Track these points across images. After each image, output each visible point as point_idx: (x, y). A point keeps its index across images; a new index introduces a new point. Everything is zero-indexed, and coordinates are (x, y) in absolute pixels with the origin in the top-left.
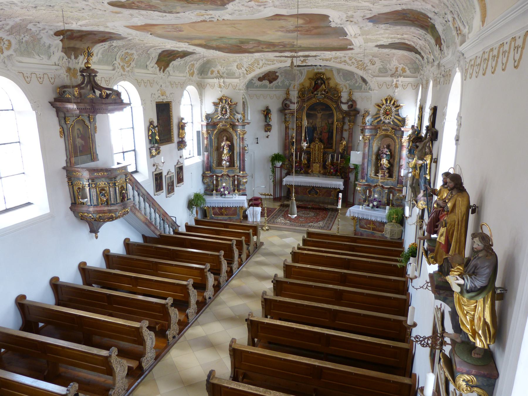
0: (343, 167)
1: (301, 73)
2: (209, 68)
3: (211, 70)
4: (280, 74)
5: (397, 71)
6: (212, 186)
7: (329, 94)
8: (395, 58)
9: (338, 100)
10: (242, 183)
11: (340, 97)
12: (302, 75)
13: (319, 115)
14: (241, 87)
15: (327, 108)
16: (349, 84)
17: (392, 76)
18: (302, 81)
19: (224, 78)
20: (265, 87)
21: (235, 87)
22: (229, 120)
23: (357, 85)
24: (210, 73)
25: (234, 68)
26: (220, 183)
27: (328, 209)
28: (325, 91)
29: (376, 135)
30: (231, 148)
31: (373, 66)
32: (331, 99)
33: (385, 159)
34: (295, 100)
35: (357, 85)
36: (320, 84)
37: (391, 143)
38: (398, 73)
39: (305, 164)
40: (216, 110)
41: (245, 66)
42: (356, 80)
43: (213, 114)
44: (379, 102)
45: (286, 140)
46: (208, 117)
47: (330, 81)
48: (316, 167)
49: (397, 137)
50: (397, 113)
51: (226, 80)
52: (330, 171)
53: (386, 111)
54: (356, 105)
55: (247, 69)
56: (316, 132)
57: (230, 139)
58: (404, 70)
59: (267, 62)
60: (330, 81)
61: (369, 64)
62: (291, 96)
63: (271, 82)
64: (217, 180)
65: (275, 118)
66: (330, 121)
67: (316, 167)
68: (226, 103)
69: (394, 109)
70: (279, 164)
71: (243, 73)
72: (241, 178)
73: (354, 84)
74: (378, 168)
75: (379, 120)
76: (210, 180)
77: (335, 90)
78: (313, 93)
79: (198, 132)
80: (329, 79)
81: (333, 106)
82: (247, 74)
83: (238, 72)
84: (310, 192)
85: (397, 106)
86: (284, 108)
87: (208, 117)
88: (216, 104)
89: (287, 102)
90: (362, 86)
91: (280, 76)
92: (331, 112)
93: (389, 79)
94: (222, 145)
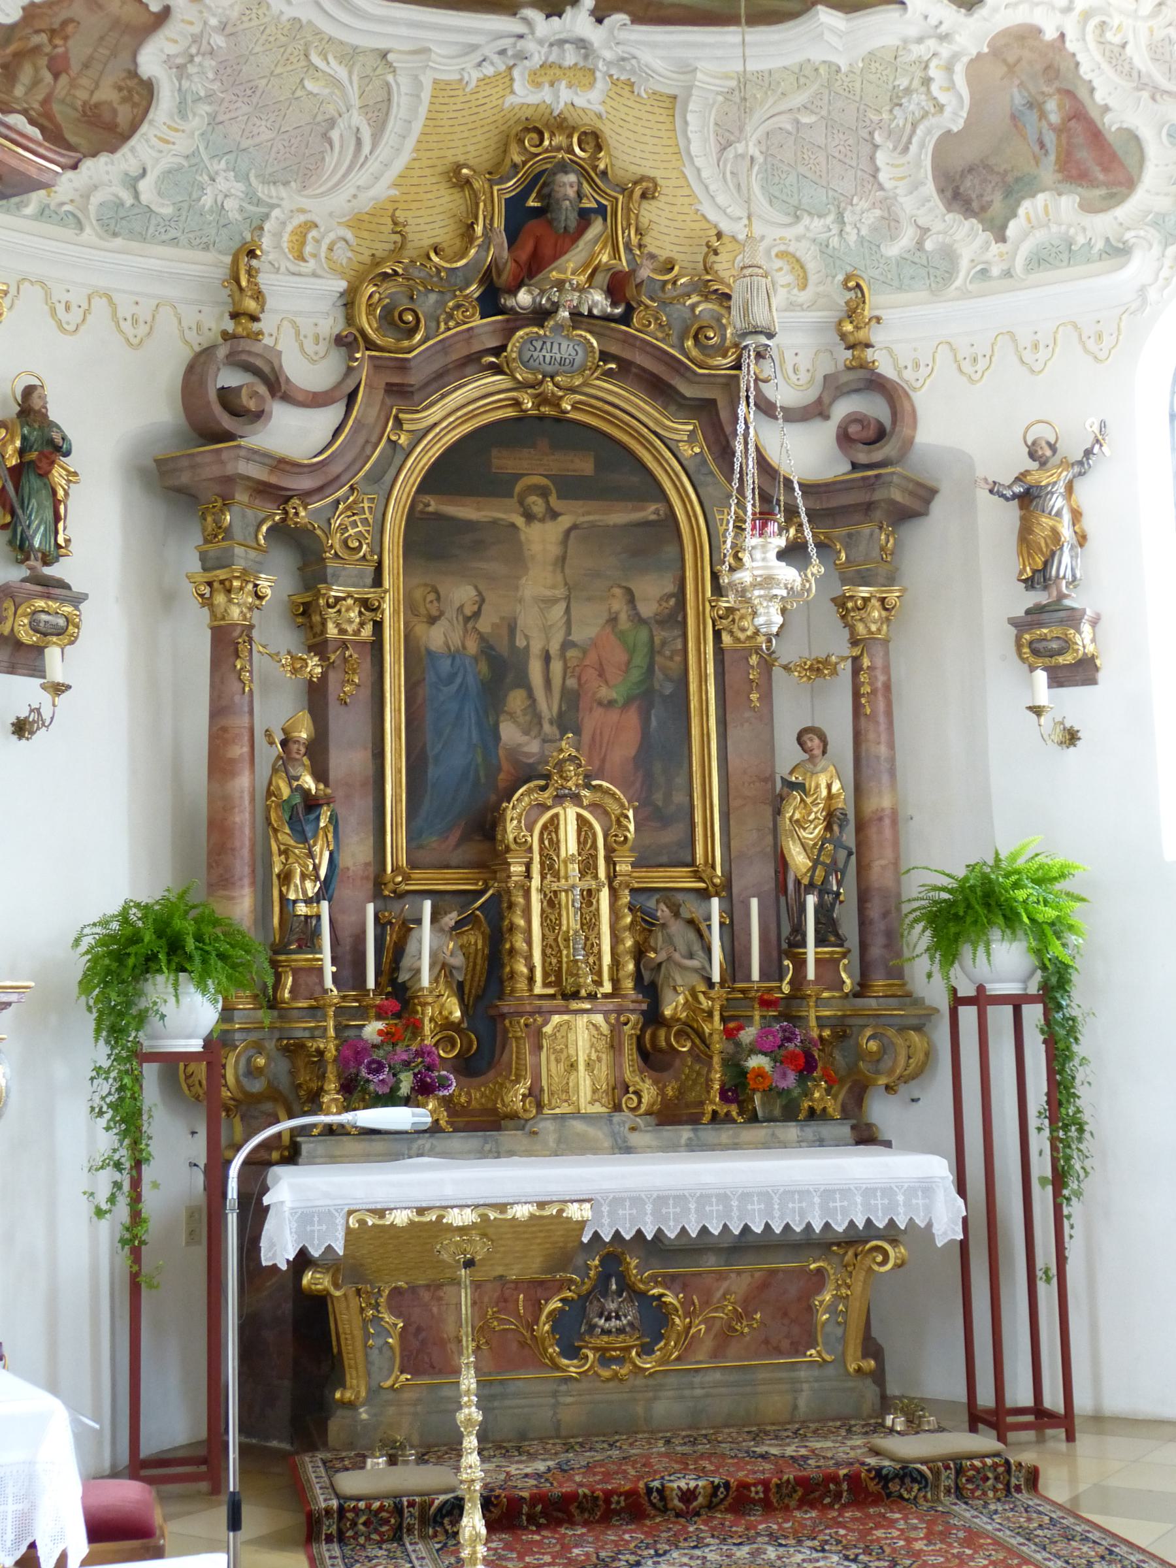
1: (379, 112)
12: (379, 129)
13: (541, 539)
15: (615, 469)
18: (382, 190)
23: (892, 250)
27: (907, 1474)
32: (658, 389)
34: (308, 364)
36: (567, 215)
45: (219, 765)
47: (649, 212)
48: (579, 1046)
56: (516, 700)
60: (649, 212)
66: (651, 592)
67: (579, 1046)
70: (188, 1015)
73: (870, 245)
84: (571, 1332)
90: (949, 255)
92: (650, 512)
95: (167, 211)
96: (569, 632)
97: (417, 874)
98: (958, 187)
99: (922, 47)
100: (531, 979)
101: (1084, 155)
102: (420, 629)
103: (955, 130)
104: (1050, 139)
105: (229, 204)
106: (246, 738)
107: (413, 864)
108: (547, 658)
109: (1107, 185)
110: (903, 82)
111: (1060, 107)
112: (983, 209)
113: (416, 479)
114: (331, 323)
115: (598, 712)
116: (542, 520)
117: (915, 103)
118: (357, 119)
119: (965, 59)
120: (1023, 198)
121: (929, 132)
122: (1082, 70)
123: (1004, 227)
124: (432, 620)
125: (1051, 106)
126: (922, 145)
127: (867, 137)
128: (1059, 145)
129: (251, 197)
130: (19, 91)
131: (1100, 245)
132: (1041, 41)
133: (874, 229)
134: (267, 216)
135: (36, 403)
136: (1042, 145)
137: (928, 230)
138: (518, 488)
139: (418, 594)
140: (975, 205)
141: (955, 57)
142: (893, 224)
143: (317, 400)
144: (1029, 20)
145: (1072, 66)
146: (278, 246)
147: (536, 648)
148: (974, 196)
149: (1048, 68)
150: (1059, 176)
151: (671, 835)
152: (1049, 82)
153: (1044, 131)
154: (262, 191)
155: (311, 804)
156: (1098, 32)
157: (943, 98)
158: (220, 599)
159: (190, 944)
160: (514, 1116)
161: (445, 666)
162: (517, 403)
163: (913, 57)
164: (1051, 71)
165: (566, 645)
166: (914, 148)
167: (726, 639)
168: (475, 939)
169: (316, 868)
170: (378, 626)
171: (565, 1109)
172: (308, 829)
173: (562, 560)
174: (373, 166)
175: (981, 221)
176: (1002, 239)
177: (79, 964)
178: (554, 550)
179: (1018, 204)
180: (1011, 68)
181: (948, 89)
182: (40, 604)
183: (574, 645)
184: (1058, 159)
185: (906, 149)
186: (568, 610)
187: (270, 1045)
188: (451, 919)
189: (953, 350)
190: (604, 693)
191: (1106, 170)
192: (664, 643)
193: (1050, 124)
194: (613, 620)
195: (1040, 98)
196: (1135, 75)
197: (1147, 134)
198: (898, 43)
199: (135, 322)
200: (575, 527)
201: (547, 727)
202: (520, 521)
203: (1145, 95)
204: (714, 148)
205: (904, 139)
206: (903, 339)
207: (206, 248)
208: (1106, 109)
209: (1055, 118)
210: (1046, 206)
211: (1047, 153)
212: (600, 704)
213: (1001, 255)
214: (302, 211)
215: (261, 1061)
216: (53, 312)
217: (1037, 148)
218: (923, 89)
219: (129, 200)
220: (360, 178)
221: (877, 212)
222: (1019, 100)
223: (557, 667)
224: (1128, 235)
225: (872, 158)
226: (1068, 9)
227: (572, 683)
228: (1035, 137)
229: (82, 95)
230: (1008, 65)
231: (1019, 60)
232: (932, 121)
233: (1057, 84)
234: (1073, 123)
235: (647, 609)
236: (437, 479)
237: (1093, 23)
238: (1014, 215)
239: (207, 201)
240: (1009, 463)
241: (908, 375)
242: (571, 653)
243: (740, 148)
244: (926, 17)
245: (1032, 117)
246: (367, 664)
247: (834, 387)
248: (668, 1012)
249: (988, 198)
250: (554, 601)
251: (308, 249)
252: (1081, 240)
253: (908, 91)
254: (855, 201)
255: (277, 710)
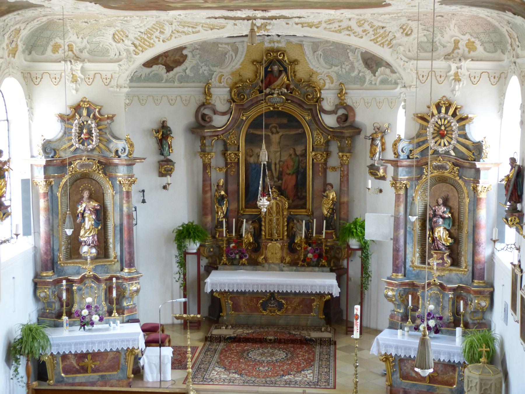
0: (332, 248)
1: (236, 51)
2: (50, 39)
3: (52, 43)
4: (191, 52)
5: (456, 47)
6: (57, 306)
7: (296, 94)
8: (454, 22)
9: (312, 103)
10: (127, 294)
11: (319, 100)
14: (121, 82)
15: (292, 122)
16: (337, 74)
17: (447, 57)
18: (238, 66)
19: (83, 61)
20: (157, 78)
21: (107, 82)
22: (96, 153)
23: (353, 75)
24: (50, 48)
25: (107, 40)
26: (77, 297)
27: (311, 340)
28: (287, 88)
29: (419, 179)
30: (101, 216)
31: (406, 39)
32: (300, 105)
33: (441, 229)
34: (221, 105)
35: (353, 75)
36: (276, 73)
37: (451, 195)
38: (460, 51)
39: (250, 244)
40: (67, 133)
41: (131, 36)
42: (352, 64)
43: (60, 140)
44: (422, 110)
45: (204, 192)
46: (48, 147)
47: (297, 68)
48: (274, 249)
49: (465, 181)
50: (461, 132)
51: (88, 65)
52: (306, 256)
53: (440, 128)
54: (354, 116)
55: (137, 43)
57: (97, 196)
58: (471, 46)
59: (181, 29)
61: (398, 35)
62: (214, 97)
63: (169, 69)
64: (69, 291)
65: (180, 147)
67: (274, 249)
68: (88, 115)
69: (455, 125)
70: (193, 247)
71: (127, 51)
72: (126, 284)
73: (348, 73)
74: (427, 247)
75: (424, 146)
76: (53, 292)
77: (309, 86)
78: (261, 92)
79: (25, 183)
80: (295, 62)
81: (305, 118)
82: (136, 54)
83: (114, 48)
84: (264, 306)
85: (462, 119)
86: (200, 125)
87: (48, 147)
88: (65, 119)
89: (207, 112)
90: (365, 78)
91: (190, 55)
92: (300, 131)
93: (440, 64)
94: (80, 209)
95: (192, 75)
96: (281, 158)
97: (247, 210)
100: (265, 236)
102: (248, 158)
105: (205, 72)
106: (209, 186)
107: (246, 208)
108: (276, 164)
113: (248, 125)
114: (227, 97)
115: (286, 176)
116: (275, 134)
118: (231, 53)
124: (251, 156)
129: (210, 70)
130: (159, 61)
131: (393, 81)
133: (349, 69)
134: (213, 74)
135: (165, 125)
138: (270, 126)
139: (248, 151)
143: (224, 114)
146: (215, 80)
147: (273, 162)
151: (301, 203)
154: (212, 68)
155: (223, 197)
158: (204, 158)
159: (192, 234)
160: (260, 263)
161: (254, 166)
162: (269, 109)
165: (280, 161)
167: (315, 160)
168: (257, 225)
169: (223, 212)
170: (239, 159)
171: (271, 262)
172: (222, 204)
173: (279, 143)
174: (236, 61)
176: (375, 76)
177: (175, 234)
178: (278, 140)
182: (166, 166)
183: (281, 161)
185: (354, 54)
186: (280, 154)
187: (214, 246)
188: (250, 222)
189: (364, 100)
190: (288, 172)
192: (302, 160)
194: (291, 155)
199: (186, 100)
200: (283, 135)
201: (275, 179)
202: (270, 134)
204: (311, 52)
206: (355, 97)
207: (200, 82)
212: (287, 174)
214: (221, 72)
215: (212, 250)
216: (169, 101)
219: (184, 74)
220: (233, 64)
223: (278, 166)
224: (398, 81)
227: (281, 169)
229: (172, 59)
235: (298, 153)
236: (251, 126)
239: (201, 72)
240: (369, 131)
241: (355, 104)
242: (281, 163)
243: (317, 53)
246: (236, 167)
247: (337, 107)
248: (296, 241)
250: (278, 152)
251: (222, 80)
252: (390, 79)
255: (218, 177)
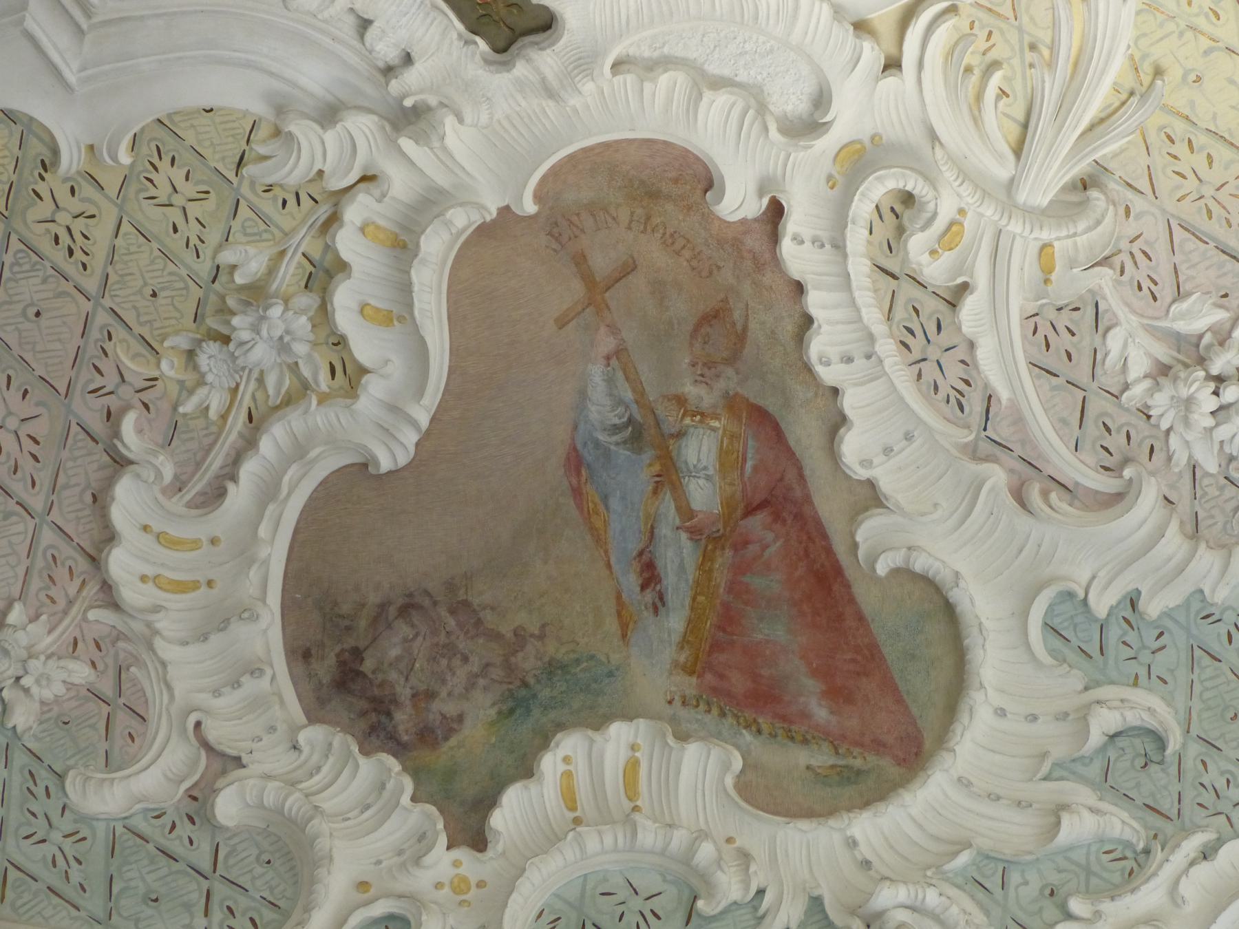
23: (106, 798)
98: (357, 654)
99: (330, 136)
101: (778, 633)
103: (385, 464)
104: (678, 558)
109: (835, 740)
110: (249, 260)
111: (728, 460)
112: (428, 736)
117: (274, 337)
119: (462, 220)
120: (560, 727)
121: (299, 451)
122: (816, 347)
123: (487, 802)
125: (700, 450)
126: (269, 492)
127: (97, 425)
128: (702, 586)
132: (709, 217)
136: (650, 575)
137: (238, 762)
140: (403, 719)
141: (430, 204)
142: (123, 721)
144: (678, 134)
145: (788, 327)
148: (404, 693)
149: (713, 317)
150: (689, 685)
152: (707, 368)
153: (665, 530)
156: (884, 231)
157: (365, 345)
163: (294, 173)
164: (719, 332)
166: (240, 496)
175: (416, 772)
176: (472, 835)
179: (544, 741)
180: (596, 291)
181: (386, 319)
184: (693, 625)
185: (216, 495)
191: (838, 695)
193: (686, 512)
195: (670, 418)
196: (975, 405)
197: (982, 605)
198: (259, 108)
203: (997, 476)
205: (216, 462)
208: (870, 497)
209: (703, 495)
210: (631, 769)
211: (659, 605)
213: (460, 885)
217: (631, 581)
218: (308, 301)
221: (81, 673)
222: (601, 410)
225: (100, 500)
226: (809, 126)
228: (634, 546)
230: (588, 279)
231: (628, 269)
232: (315, 417)
233: (729, 381)
234: (757, 522)
237: (877, 189)
238: (526, 770)
244: (364, 24)
245: (633, 475)
249: (451, 709)
252: (731, 887)
253: (256, 294)
254: (16, 615)
